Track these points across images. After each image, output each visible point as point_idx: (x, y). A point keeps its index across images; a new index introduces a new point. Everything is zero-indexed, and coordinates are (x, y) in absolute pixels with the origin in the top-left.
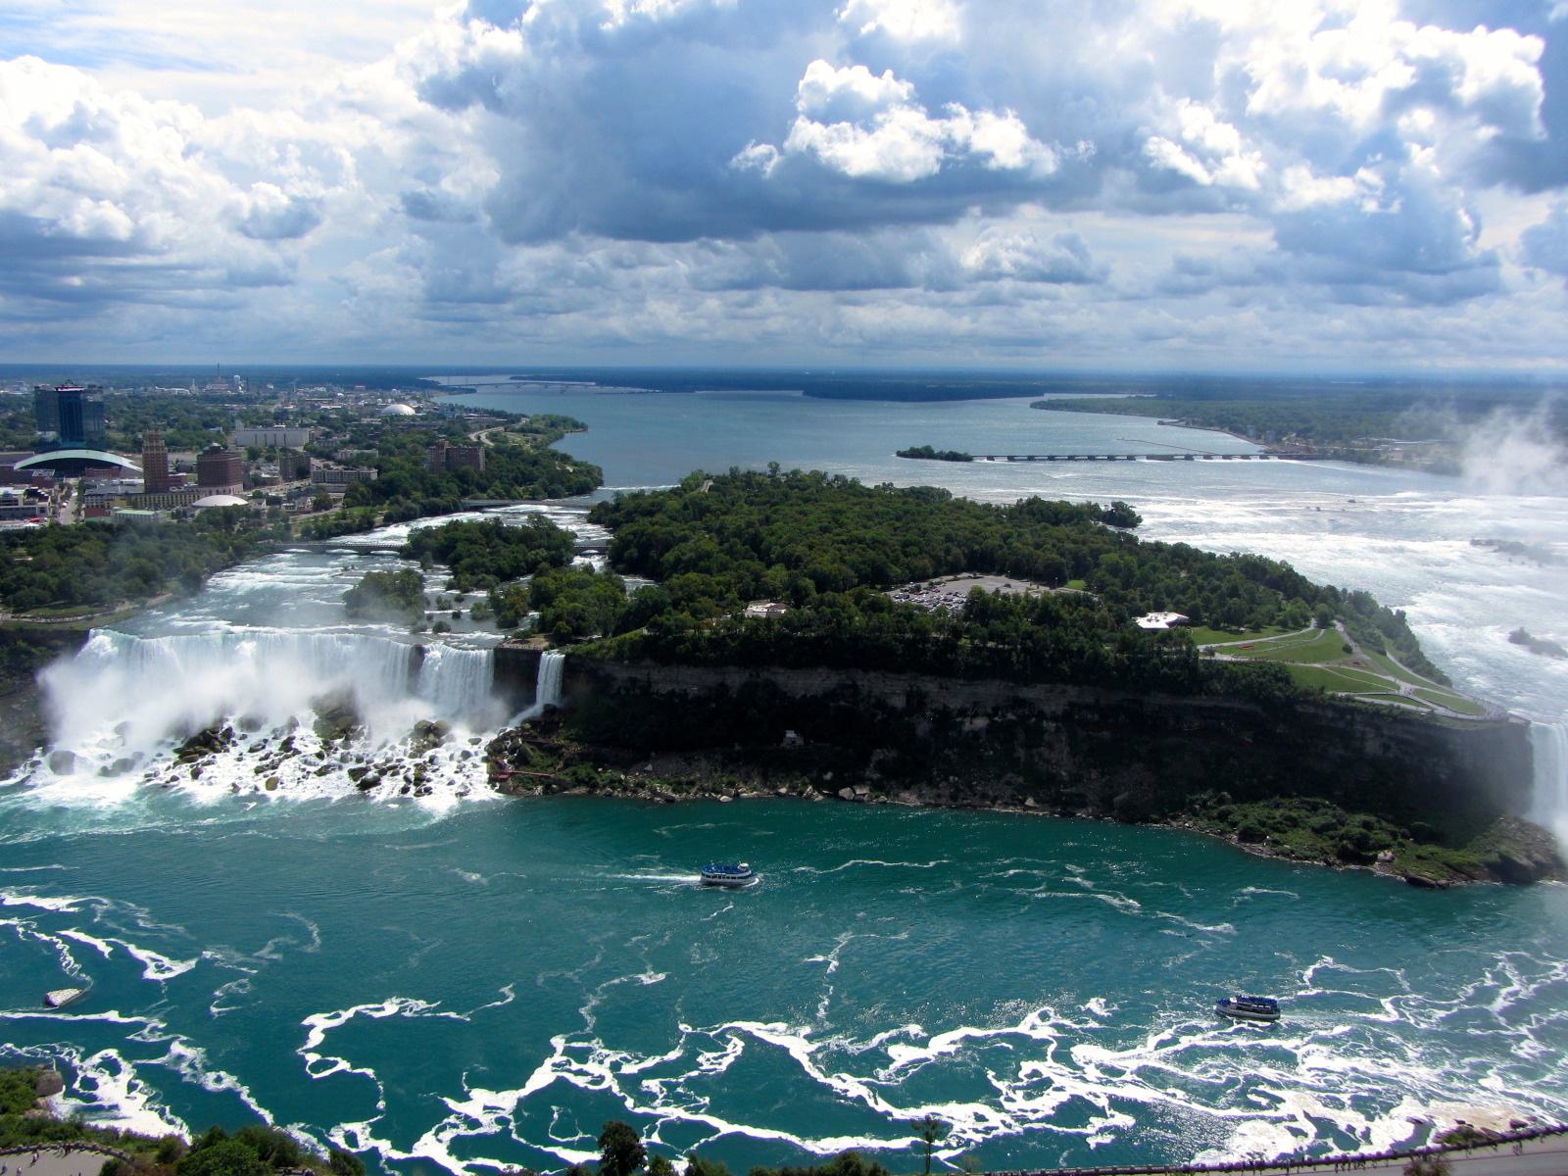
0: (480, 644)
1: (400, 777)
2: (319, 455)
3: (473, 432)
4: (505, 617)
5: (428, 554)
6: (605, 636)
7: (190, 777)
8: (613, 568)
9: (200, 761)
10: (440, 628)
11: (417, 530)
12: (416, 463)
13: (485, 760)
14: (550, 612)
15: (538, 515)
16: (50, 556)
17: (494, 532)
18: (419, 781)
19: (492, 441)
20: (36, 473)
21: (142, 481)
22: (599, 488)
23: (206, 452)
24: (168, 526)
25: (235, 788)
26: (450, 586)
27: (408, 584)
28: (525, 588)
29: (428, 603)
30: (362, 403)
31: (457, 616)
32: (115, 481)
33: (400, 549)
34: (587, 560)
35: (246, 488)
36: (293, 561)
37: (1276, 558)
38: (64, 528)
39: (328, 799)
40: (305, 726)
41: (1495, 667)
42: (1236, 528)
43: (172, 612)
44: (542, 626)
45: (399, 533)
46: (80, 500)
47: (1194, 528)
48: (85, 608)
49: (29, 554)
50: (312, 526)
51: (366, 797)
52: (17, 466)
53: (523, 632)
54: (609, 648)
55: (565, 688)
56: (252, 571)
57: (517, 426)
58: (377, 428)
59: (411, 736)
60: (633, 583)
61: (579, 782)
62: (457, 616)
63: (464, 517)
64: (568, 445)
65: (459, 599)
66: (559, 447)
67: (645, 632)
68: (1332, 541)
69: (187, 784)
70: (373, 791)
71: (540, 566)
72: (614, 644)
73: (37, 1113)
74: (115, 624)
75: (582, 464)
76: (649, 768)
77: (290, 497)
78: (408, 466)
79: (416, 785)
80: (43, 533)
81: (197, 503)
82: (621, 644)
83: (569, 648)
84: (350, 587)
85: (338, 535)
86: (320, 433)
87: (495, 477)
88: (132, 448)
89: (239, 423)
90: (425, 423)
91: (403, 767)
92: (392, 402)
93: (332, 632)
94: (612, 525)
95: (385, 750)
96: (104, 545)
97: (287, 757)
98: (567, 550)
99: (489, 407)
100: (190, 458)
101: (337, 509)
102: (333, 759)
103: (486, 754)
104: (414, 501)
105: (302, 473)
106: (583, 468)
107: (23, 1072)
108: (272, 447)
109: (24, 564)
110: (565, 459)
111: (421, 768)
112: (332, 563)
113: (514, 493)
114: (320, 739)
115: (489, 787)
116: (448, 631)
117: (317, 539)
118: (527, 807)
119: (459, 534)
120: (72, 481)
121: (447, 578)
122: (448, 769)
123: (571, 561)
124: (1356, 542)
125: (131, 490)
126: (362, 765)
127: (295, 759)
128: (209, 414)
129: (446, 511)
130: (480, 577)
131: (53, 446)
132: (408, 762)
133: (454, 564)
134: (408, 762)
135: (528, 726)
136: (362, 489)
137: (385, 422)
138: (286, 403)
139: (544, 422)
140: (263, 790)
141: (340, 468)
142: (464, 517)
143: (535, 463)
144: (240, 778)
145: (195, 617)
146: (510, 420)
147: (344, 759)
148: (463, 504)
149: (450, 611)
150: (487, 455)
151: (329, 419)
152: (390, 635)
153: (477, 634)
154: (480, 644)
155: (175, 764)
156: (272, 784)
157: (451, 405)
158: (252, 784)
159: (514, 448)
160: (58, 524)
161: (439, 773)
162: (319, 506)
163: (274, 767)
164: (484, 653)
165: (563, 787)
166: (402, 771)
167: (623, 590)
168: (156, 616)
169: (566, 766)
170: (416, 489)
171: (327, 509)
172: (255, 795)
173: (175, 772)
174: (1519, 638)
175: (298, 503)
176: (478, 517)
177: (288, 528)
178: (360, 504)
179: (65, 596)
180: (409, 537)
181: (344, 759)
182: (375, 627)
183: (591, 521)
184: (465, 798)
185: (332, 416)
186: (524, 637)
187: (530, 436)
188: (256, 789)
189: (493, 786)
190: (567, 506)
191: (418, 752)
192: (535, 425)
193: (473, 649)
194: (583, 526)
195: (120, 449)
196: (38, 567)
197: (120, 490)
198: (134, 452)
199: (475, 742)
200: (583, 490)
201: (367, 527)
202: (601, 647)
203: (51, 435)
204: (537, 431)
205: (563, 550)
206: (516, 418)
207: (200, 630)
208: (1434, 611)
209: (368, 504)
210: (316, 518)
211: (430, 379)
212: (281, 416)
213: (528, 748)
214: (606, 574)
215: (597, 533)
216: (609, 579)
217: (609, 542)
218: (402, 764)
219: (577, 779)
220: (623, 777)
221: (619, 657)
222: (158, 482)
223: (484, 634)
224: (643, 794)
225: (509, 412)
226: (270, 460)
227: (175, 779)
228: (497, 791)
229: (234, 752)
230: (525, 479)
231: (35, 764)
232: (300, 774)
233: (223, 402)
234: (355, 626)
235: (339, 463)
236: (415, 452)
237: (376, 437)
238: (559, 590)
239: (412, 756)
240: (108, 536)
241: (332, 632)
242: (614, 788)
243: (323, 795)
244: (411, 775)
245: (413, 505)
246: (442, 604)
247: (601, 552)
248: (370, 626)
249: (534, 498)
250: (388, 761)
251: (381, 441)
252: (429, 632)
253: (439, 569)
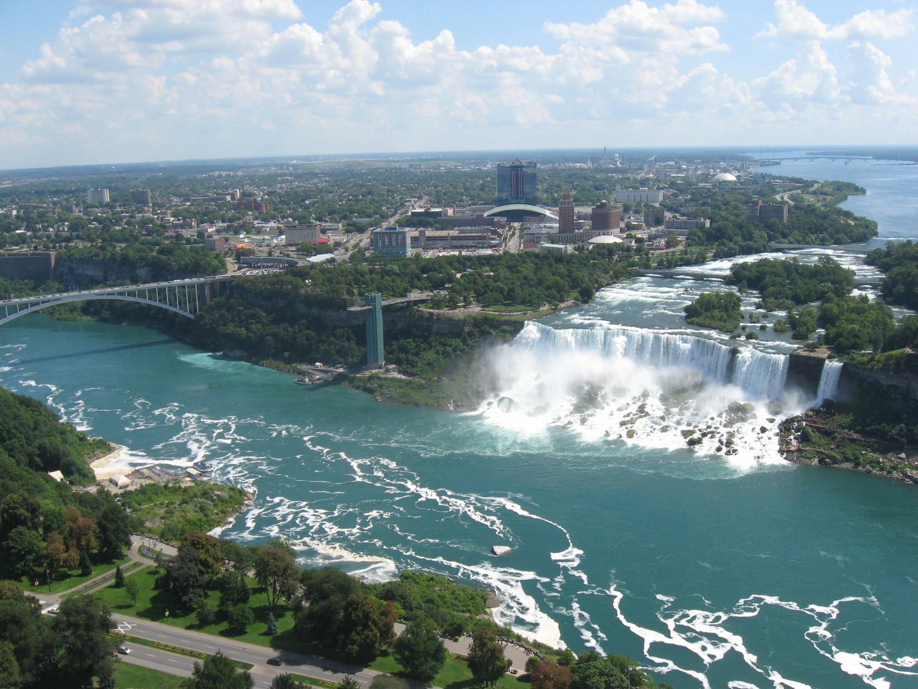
1: (716, 439)
2: (670, 209)
3: (778, 194)
4: (799, 332)
5: (745, 282)
6: (875, 349)
7: (579, 423)
8: (884, 299)
9: (586, 413)
10: (750, 337)
11: (737, 264)
12: (737, 216)
13: (777, 435)
14: (833, 331)
15: (827, 257)
16: (504, 273)
18: (729, 443)
19: (792, 200)
20: (496, 219)
21: (557, 225)
22: (874, 238)
23: (598, 207)
24: (572, 255)
25: (607, 434)
26: (758, 306)
27: (730, 303)
29: (743, 317)
30: (699, 172)
31: (763, 328)
32: (542, 225)
33: (724, 278)
34: (864, 293)
35: (622, 231)
36: (652, 282)
38: (513, 255)
39: (666, 449)
40: (653, 397)
43: (574, 313)
44: (827, 340)
45: (724, 266)
46: (521, 237)
48: (522, 307)
49: (491, 271)
50: (665, 259)
51: (691, 451)
52: (485, 215)
53: (812, 344)
54: (879, 361)
55: (840, 384)
56: (624, 288)
57: (811, 190)
58: (709, 190)
59: (726, 411)
60: (899, 313)
61: (847, 460)
62: (763, 328)
63: (770, 256)
64: (851, 204)
65: (765, 316)
66: (844, 206)
67: (908, 350)
69: (577, 428)
70: (697, 447)
71: (827, 296)
72: (883, 358)
73: (486, 617)
74: (539, 319)
75: (863, 219)
76: (903, 455)
77: (651, 238)
78: (732, 217)
79: (726, 446)
80: (500, 258)
81: (591, 241)
82: (888, 358)
83: (846, 358)
84: (690, 303)
85: (681, 266)
86: (670, 193)
87: (794, 228)
88: (552, 203)
89: (618, 187)
90: (743, 187)
91: (719, 433)
92: (720, 172)
93: (676, 334)
94: (884, 268)
95: (706, 420)
96: (534, 267)
97: (641, 417)
98: (848, 284)
99: (790, 176)
100: (587, 210)
101: (680, 247)
102: (670, 422)
103: (778, 431)
104: (735, 243)
105: (658, 221)
106: (861, 222)
107: (479, 591)
108: (639, 203)
109: (488, 276)
110: (848, 214)
111: (731, 435)
112: (676, 285)
113: (808, 239)
114: (663, 407)
115: (779, 454)
116: (756, 338)
117: (667, 268)
118: (805, 470)
119: (767, 269)
120: (516, 225)
121: (757, 300)
122: (751, 437)
123: (850, 291)
125: (551, 231)
126: (691, 428)
127: (645, 419)
128: (598, 180)
129: (757, 251)
130: (781, 301)
131: (506, 202)
132: (723, 430)
133: (762, 290)
134: (723, 430)
135: (811, 413)
136: (700, 234)
137: (714, 186)
138: (647, 173)
139: (832, 187)
140: (625, 438)
141: (684, 218)
142: (770, 256)
143: (825, 218)
144: (611, 428)
145: (587, 317)
146: (806, 185)
147: (678, 423)
148: (770, 247)
149: (759, 325)
150: (789, 211)
151: (676, 184)
152: (715, 339)
153: (777, 343)
154: (779, 350)
155: (571, 413)
156: (630, 434)
157: (762, 174)
158: (618, 432)
159: (809, 206)
160: (508, 252)
161: (743, 440)
162: (668, 245)
163: (632, 422)
164: (782, 358)
165: (835, 461)
166: (717, 436)
167: (891, 317)
168: (563, 316)
169: (838, 446)
170: (736, 235)
171: (674, 247)
172: (619, 442)
173: (570, 419)
175: (656, 242)
176: (780, 256)
177: (648, 259)
178: (698, 245)
179: (509, 298)
180: (731, 269)
181: (678, 423)
182: (706, 332)
183: (868, 262)
184: (761, 460)
185: (679, 182)
186: (812, 347)
187: (821, 197)
188: (621, 436)
189: (782, 454)
190: (848, 251)
191: (729, 423)
192: (825, 189)
193: (774, 353)
194: (861, 267)
195: (545, 204)
196: (496, 279)
197: (544, 231)
198: (552, 206)
199: (772, 421)
200: (863, 239)
201: (701, 261)
202: (872, 359)
203: (504, 195)
204: (826, 194)
205: (844, 284)
206: (812, 183)
207: (592, 326)
209: (702, 245)
210: (667, 253)
211: (746, 155)
212: (644, 182)
213: (810, 430)
214: (877, 303)
216: (882, 309)
217: (881, 279)
218: (718, 431)
219: (845, 457)
220: (881, 460)
221: (885, 368)
222: (568, 224)
223: (783, 343)
224: (895, 474)
225: (805, 179)
226: (637, 212)
227: (570, 423)
228: (786, 458)
229: (607, 410)
230: (817, 229)
231: (490, 404)
232: (649, 429)
233: (608, 173)
234: (692, 331)
235: (683, 215)
236: (736, 208)
237: (709, 196)
238: (842, 314)
239: (725, 426)
240: (537, 261)
241: (676, 334)
242: (872, 467)
243: (663, 447)
244: (724, 440)
245: (734, 246)
246: (752, 318)
247: (874, 287)
248: (702, 331)
249: (823, 243)
250: (709, 427)
251: (712, 200)
252: (743, 338)
253: (751, 293)
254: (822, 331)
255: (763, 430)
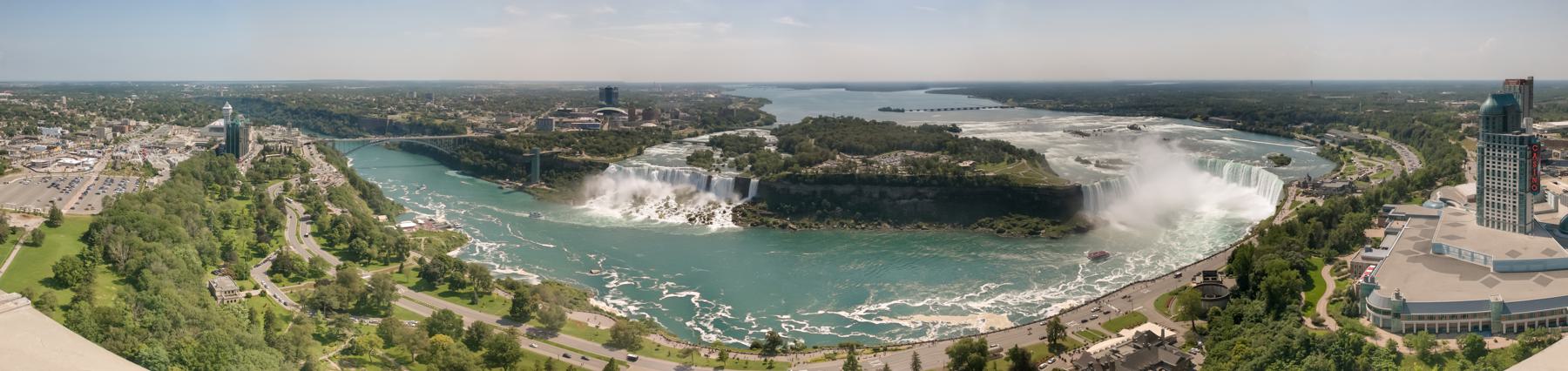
0: (731, 176)
17: (737, 138)
28: (746, 157)
37: (1005, 140)
41: (1070, 168)
42: (993, 132)
47: (980, 132)
68: (1023, 134)
94: (778, 136)
124: (1030, 134)
154: (731, 176)
174: (1078, 159)
208: (1053, 153)
215: (774, 139)
254: (750, 166)
255: (724, 212)
